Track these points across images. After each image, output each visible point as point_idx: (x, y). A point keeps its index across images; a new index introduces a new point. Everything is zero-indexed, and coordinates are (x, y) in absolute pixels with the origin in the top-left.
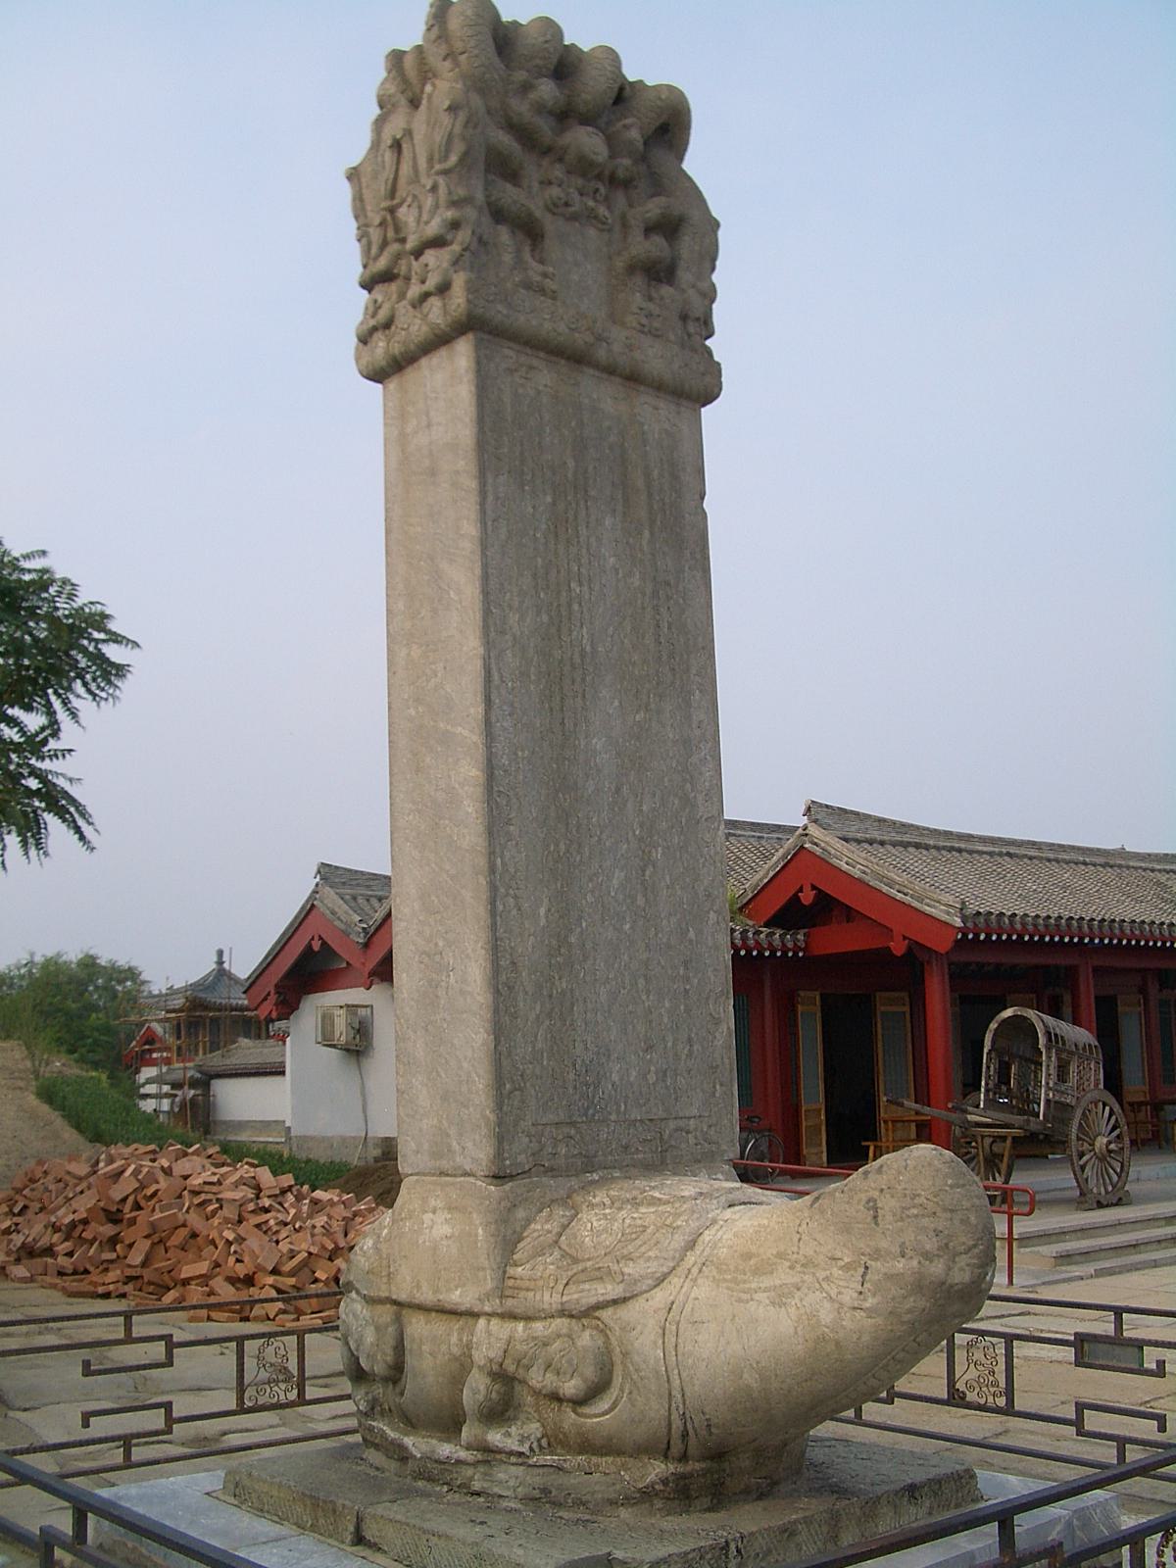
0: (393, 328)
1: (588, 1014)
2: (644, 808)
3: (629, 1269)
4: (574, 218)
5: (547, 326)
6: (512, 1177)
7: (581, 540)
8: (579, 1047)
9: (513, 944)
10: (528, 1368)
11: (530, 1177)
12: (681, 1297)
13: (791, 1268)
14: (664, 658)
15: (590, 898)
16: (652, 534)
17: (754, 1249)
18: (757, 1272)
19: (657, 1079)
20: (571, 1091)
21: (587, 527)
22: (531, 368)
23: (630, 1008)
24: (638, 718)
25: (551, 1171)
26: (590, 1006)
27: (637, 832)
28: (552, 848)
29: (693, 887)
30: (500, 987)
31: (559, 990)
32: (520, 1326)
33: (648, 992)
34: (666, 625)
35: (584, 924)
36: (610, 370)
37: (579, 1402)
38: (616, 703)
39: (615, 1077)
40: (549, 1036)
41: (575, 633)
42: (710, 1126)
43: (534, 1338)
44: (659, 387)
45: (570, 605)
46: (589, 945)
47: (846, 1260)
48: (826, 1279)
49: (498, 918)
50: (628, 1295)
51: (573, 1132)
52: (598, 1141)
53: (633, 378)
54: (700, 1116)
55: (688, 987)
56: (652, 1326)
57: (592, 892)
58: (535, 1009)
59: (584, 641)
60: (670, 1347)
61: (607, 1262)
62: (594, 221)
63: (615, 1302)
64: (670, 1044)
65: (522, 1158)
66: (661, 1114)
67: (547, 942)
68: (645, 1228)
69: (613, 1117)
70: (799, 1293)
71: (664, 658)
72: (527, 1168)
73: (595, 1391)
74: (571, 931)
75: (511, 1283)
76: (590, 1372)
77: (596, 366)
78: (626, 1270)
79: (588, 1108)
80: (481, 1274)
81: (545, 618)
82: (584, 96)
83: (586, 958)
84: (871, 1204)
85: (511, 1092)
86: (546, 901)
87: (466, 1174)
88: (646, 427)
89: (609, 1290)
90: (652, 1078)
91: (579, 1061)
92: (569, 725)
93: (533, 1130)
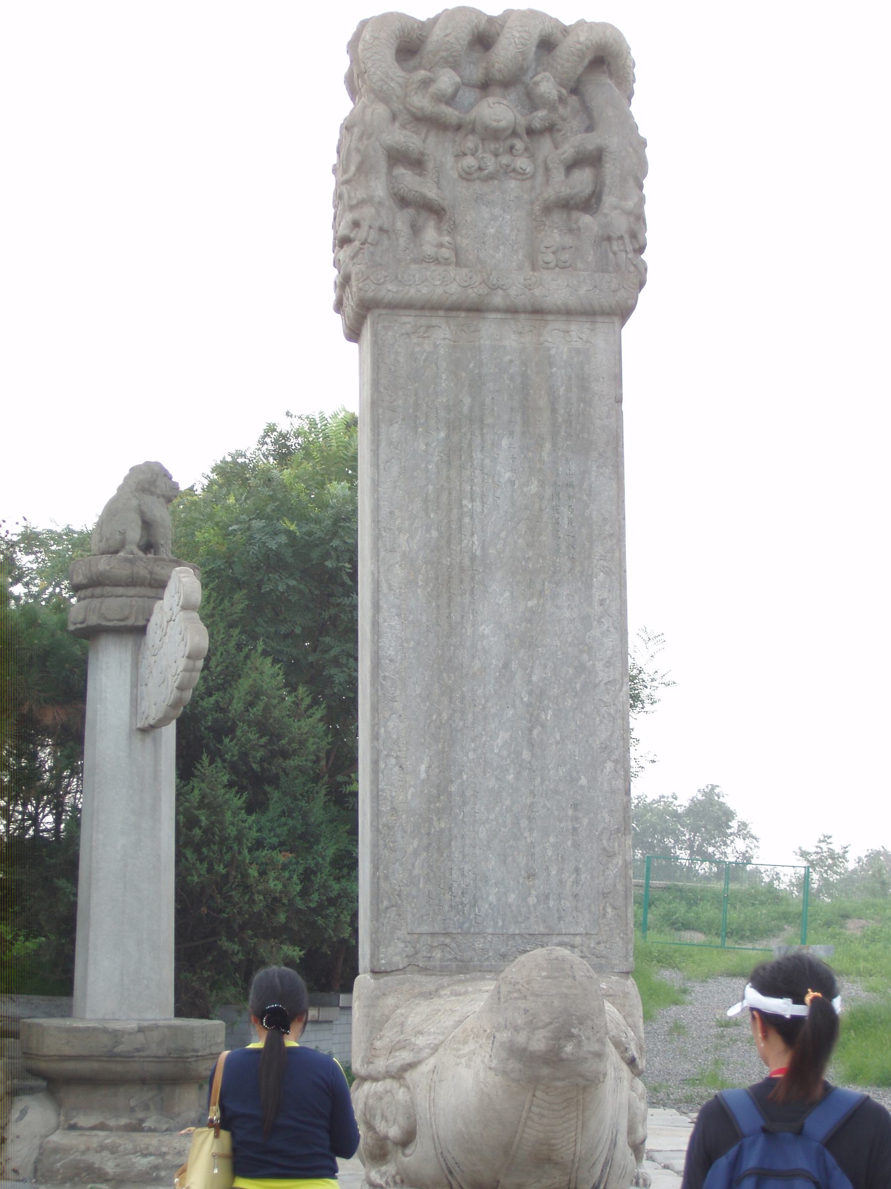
1: (467, 848)
2: (535, 678)
4: (491, 177)
5: (439, 291)
6: (386, 973)
7: (475, 462)
8: (456, 875)
9: (394, 794)
11: (405, 974)
14: (564, 548)
15: (471, 755)
16: (554, 445)
19: (538, 902)
20: (447, 908)
21: (482, 451)
22: (429, 327)
23: (511, 842)
24: (530, 604)
25: (425, 971)
26: (468, 841)
27: (526, 699)
28: (434, 717)
29: (587, 741)
30: (380, 827)
31: (438, 829)
33: (531, 830)
34: (566, 521)
35: (465, 777)
36: (512, 311)
38: (507, 594)
39: (492, 898)
40: (426, 865)
41: (465, 542)
42: (599, 943)
44: (568, 313)
45: (460, 519)
46: (469, 793)
49: (381, 775)
50: (416, 1060)
51: (448, 941)
52: (474, 950)
53: (538, 312)
54: (586, 934)
55: (577, 826)
57: (475, 750)
58: (412, 844)
59: (475, 547)
62: (512, 175)
64: (554, 873)
65: (396, 959)
66: (542, 929)
67: (426, 791)
69: (490, 930)
71: (564, 548)
72: (401, 966)
74: (452, 782)
77: (497, 310)
79: (463, 923)
81: (434, 534)
82: (497, 66)
83: (465, 803)
85: (387, 908)
86: (426, 760)
88: (553, 352)
89: (405, 1056)
90: (532, 900)
91: (455, 885)
92: (455, 617)
93: (408, 938)
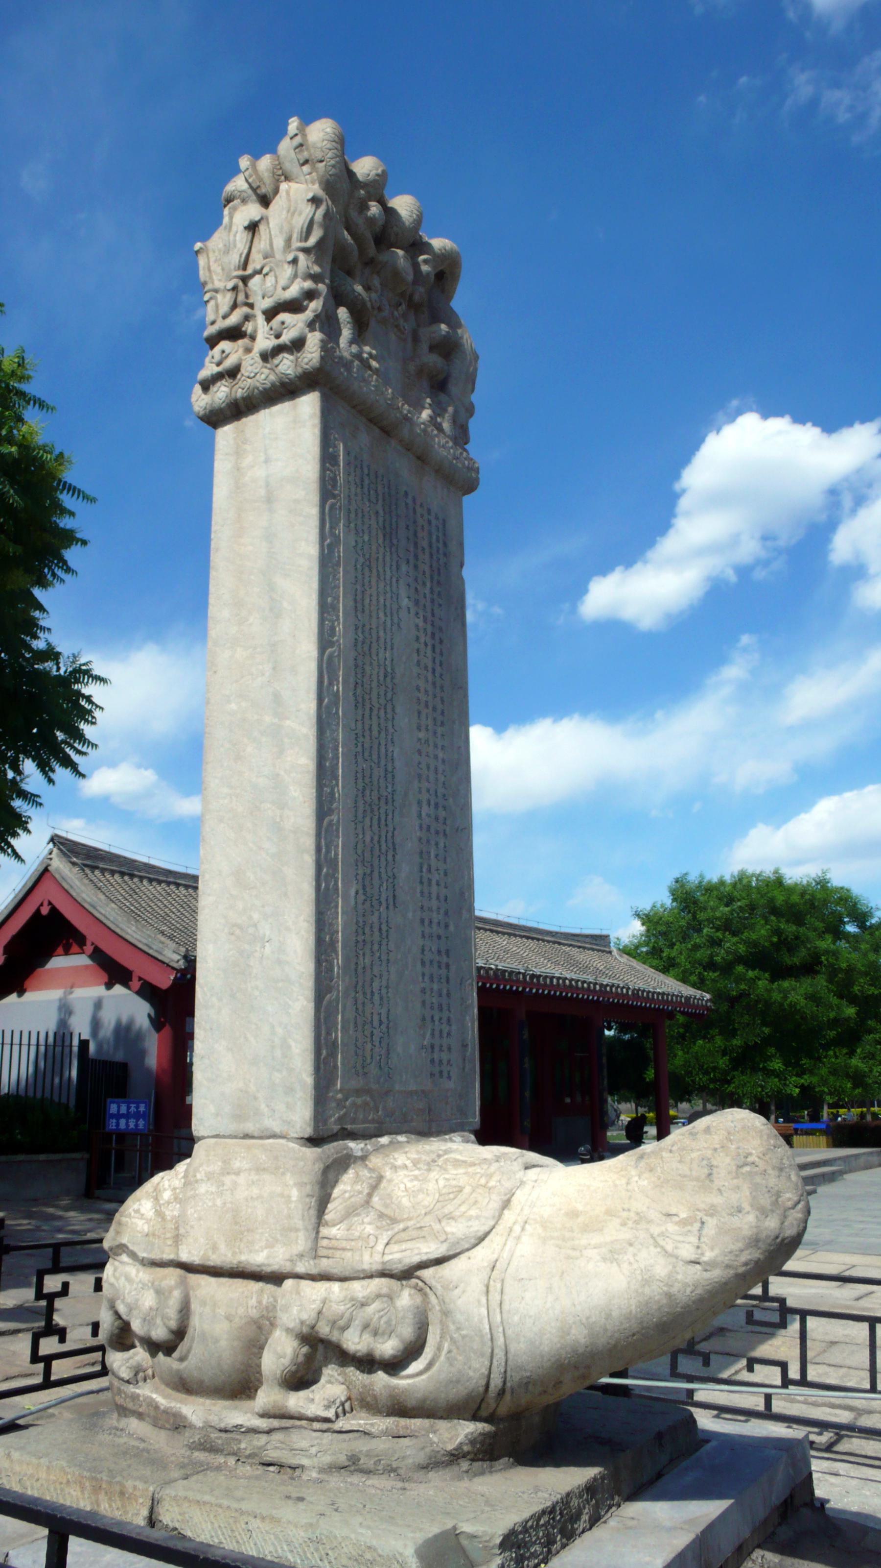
0: (239, 376)
10: (344, 1329)
12: (505, 1254)
13: (624, 1224)
17: (580, 1207)
18: (586, 1229)
32: (336, 1286)
37: (394, 1366)
43: (352, 1299)
47: (683, 1215)
48: (662, 1234)
56: (476, 1285)
60: (494, 1303)
61: (428, 1221)
63: (439, 1261)
68: (461, 1190)
70: (631, 1249)
73: (413, 1350)
75: (325, 1243)
76: (407, 1332)
78: (448, 1229)
80: (293, 1235)
82: (395, 229)
84: (705, 1162)
87: (274, 1136)
89: (430, 1249)
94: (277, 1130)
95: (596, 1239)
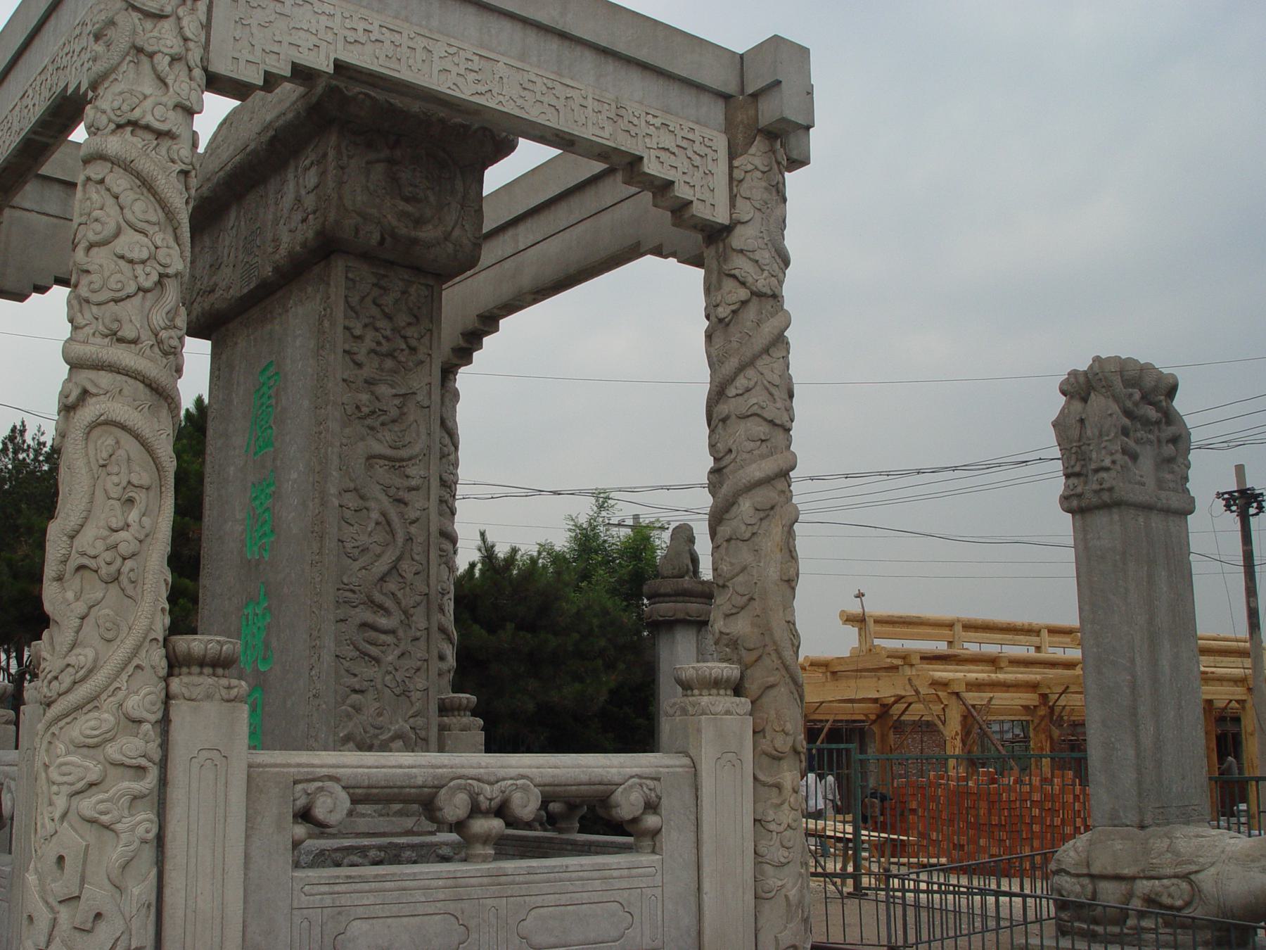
3: (1201, 860)
10: (1160, 896)
18: (1253, 861)
25: (1158, 825)
32: (1157, 882)
76: (1186, 897)
87: (1127, 826)
89: (1194, 868)
94: (1129, 823)
95: (1257, 864)
